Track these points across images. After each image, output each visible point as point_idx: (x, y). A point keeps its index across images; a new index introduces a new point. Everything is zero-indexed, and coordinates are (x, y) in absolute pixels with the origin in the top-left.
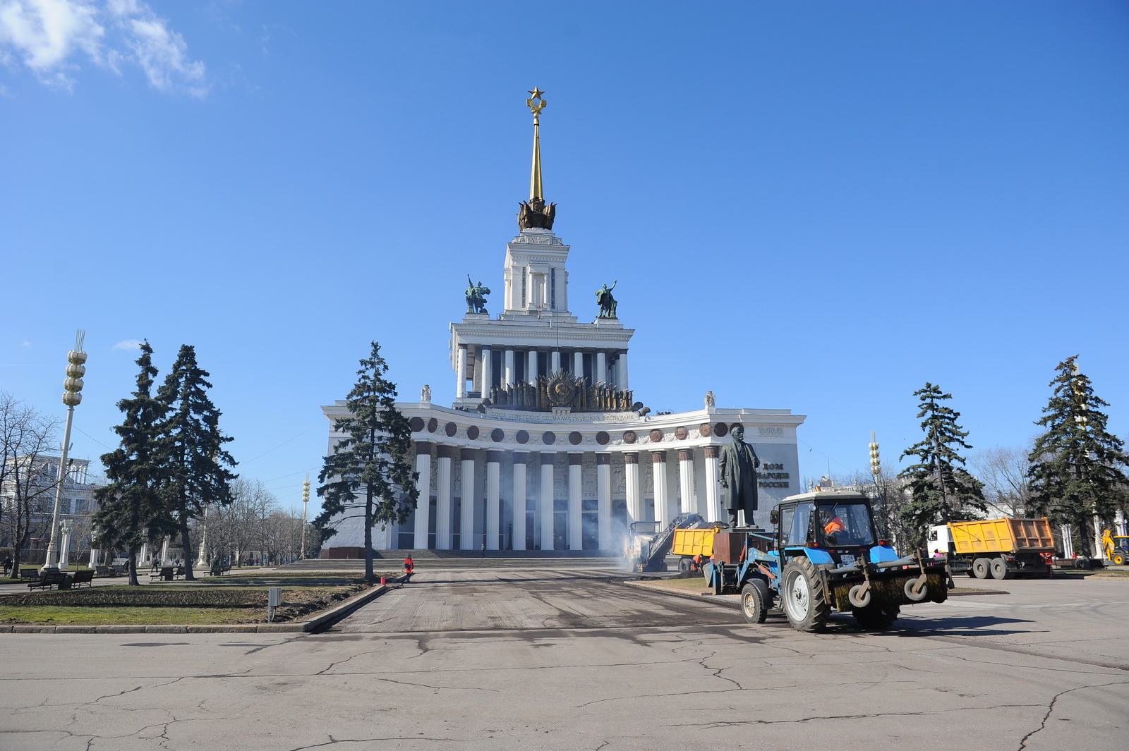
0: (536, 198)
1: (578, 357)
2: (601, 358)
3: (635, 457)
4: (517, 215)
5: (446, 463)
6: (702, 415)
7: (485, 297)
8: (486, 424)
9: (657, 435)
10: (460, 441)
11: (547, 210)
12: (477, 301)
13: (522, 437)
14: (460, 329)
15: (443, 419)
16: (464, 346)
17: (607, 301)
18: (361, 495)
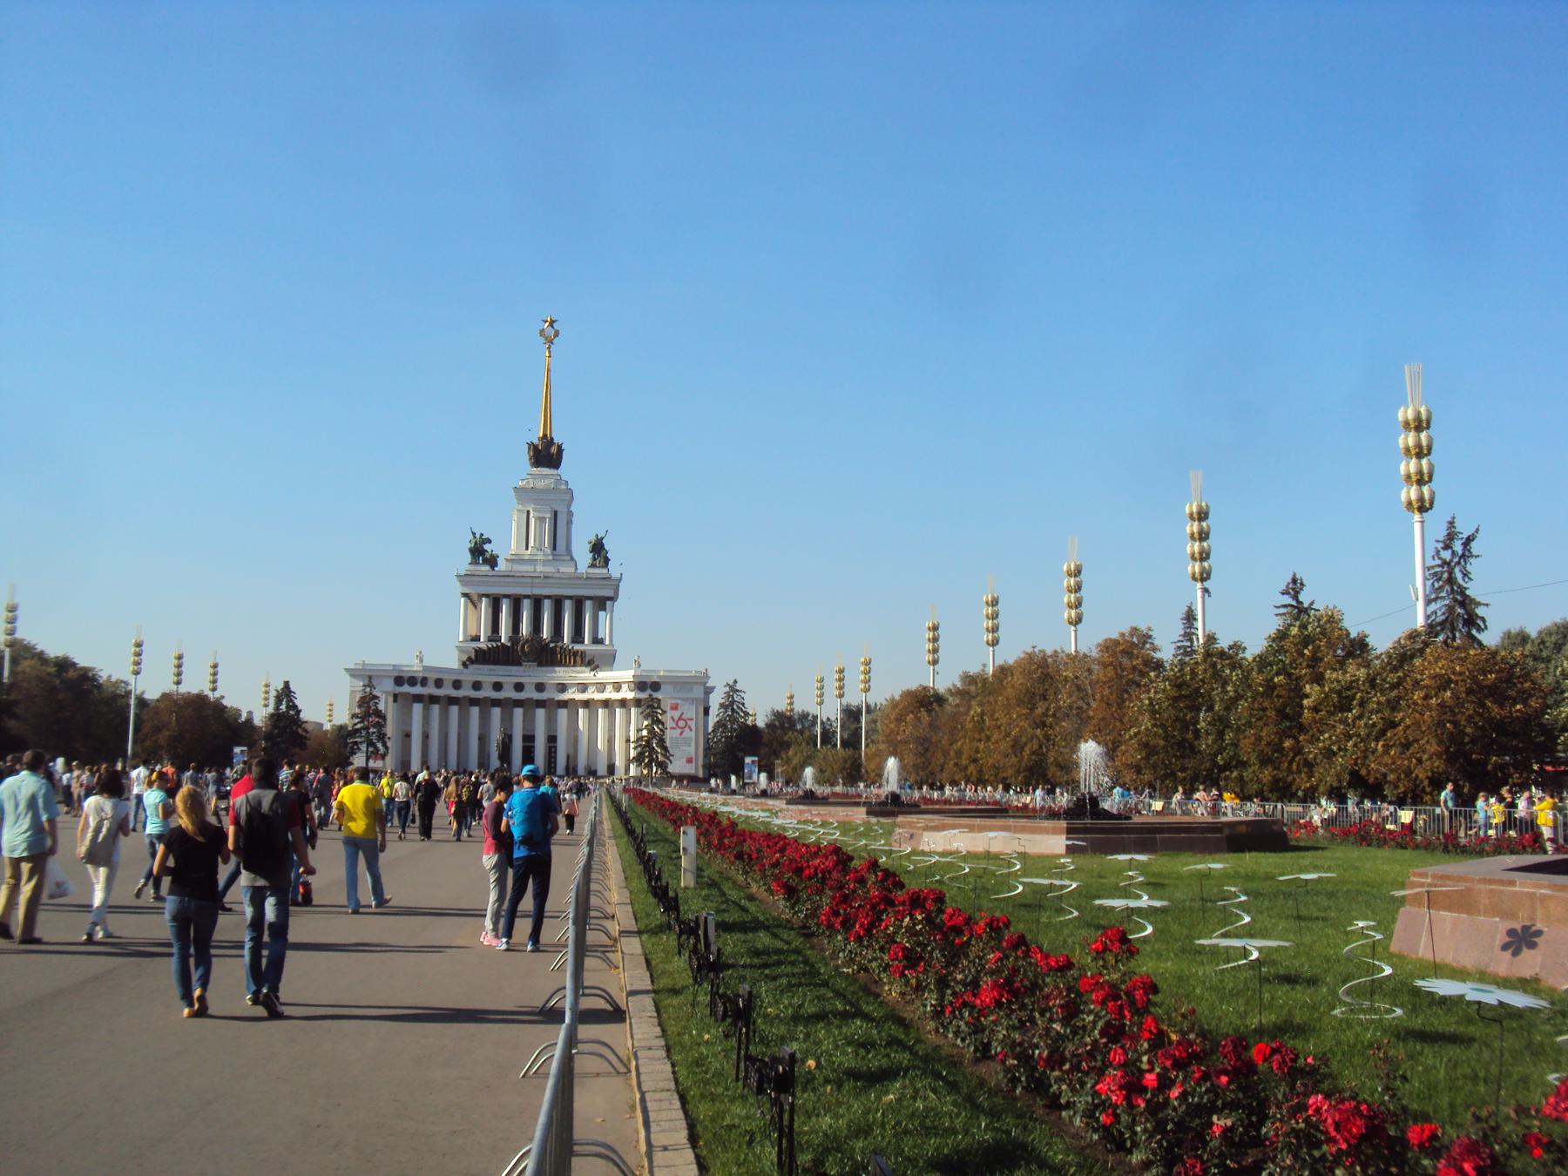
0: (545, 436)
1: (568, 605)
2: (588, 605)
3: (586, 704)
4: (524, 457)
5: (436, 708)
6: (627, 675)
7: (487, 547)
8: (470, 675)
9: (601, 687)
10: (447, 691)
11: (554, 450)
12: (479, 551)
13: (498, 686)
14: (464, 579)
15: (433, 676)
16: (465, 595)
17: (598, 548)
18: (363, 747)
